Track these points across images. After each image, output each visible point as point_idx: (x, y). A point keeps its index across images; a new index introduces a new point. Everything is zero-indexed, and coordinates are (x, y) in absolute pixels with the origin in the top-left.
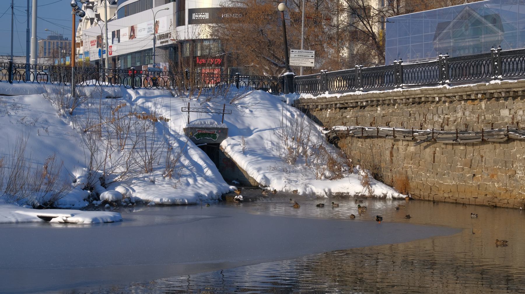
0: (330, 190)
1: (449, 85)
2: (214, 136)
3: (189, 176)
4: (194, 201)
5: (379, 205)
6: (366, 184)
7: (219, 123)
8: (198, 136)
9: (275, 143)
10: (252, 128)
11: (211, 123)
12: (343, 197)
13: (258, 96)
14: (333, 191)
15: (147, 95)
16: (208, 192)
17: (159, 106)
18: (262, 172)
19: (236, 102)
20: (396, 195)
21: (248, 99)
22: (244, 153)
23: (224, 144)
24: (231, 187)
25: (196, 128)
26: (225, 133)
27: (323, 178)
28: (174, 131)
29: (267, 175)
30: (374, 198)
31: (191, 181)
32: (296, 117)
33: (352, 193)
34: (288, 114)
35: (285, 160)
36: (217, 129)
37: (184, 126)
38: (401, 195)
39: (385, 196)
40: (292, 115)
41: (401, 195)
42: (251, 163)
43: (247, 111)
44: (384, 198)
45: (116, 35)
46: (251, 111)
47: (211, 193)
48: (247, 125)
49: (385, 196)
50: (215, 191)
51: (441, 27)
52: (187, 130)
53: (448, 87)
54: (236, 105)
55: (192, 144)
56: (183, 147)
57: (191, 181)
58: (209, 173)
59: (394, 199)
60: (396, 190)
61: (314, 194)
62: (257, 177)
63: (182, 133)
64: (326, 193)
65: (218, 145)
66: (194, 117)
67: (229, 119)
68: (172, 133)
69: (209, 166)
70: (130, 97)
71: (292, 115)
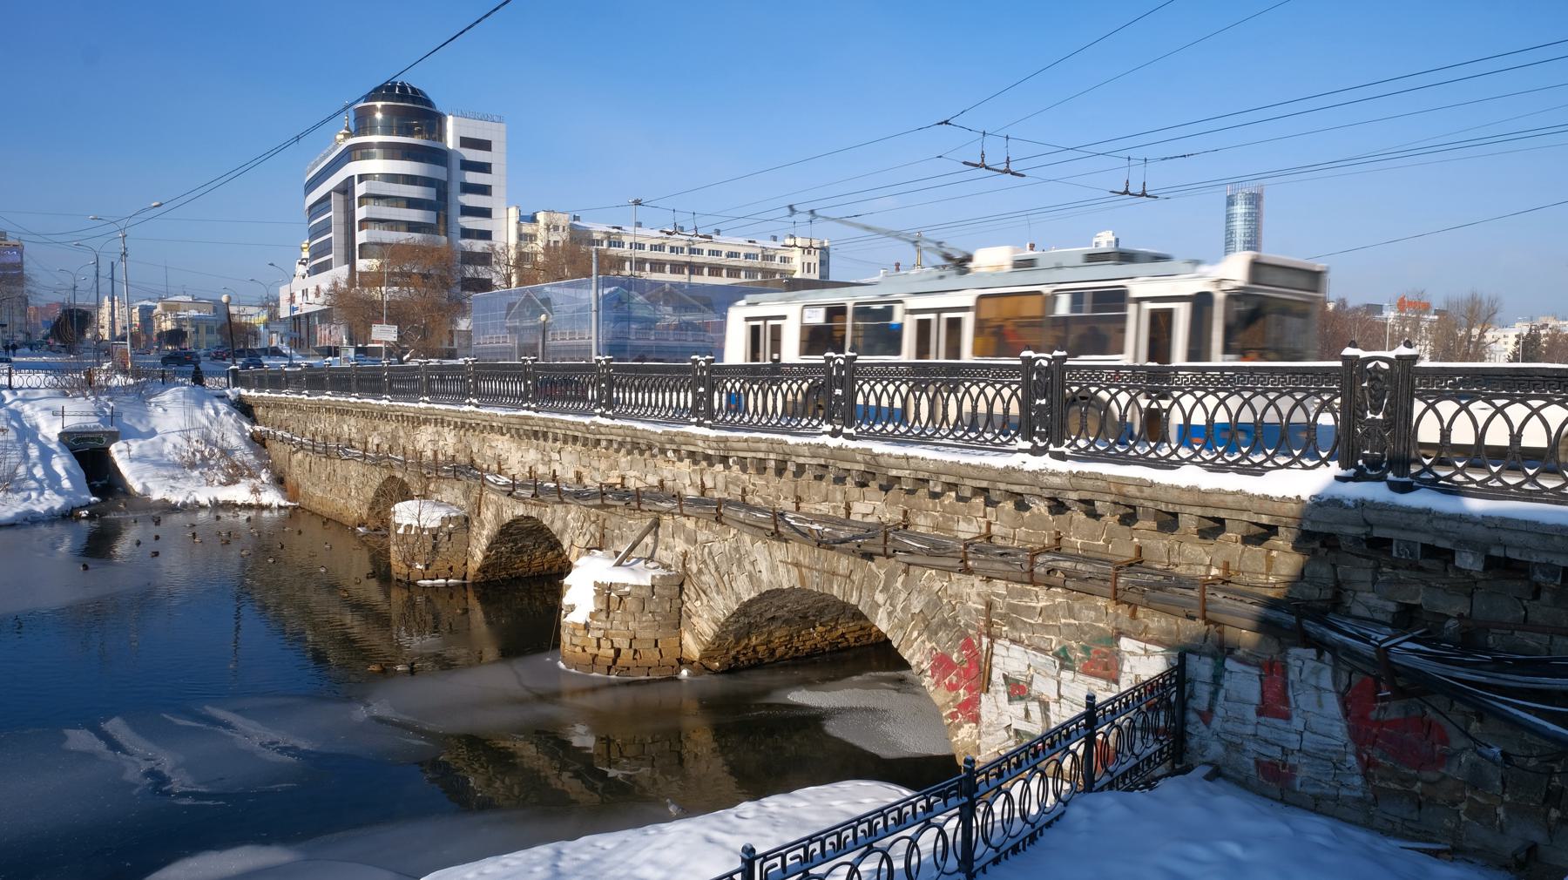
0: (215, 498)
1: (308, 396)
2: (100, 440)
3: (35, 489)
4: (13, 522)
5: (266, 514)
6: (255, 491)
7: (105, 427)
8: (77, 441)
9: (178, 446)
10: (158, 430)
11: (95, 427)
12: (229, 506)
13: (180, 394)
14: (219, 499)
15: (28, 397)
16: (46, 508)
17: (37, 409)
18: (142, 480)
19: (152, 400)
20: (283, 503)
21: (168, 396)
22: (131, 459)
23: (113, 448)
24: (93, 499)
25: (72, 433)
26: (114, 437)
27: (216, 483)
28: (44, 437)
29: (149, 485)
30: (261, 507)
31: (34, 495)
32: (222, 414)
33: (239, 502)
34: (212, 412)
35: (181, 466)
36: (103, 432)
37: (59, 430)
38: (288, 504)
39: (271, 504)
40: (217, 412)
41: (288, 504)
42: (133, 472)
43: (160, 410)
44: (268, 507)
45: (305, 292)
46: (165, 410)
47: (51, 509)
48: (152, 426)
49: (271, 504)
50: (57, 507)
51: (511, 306)
52: (61, 435)
53: (306, 397)
54: (150, 403)
55: (63, 451)
56: (46, 454)
57: (34, 495)
58: (66, 484)
59: (280, 507)
60: (284, 498)
61: (197, 502)
62: (137, 487)
63: (56, 439)
64: (210, 502)
65: (106, 451)
66: (71, 422)
67: (130, 420)
68: (40, 438)
69: (70, 477)
70: (4, 399)
71: (217, 412)
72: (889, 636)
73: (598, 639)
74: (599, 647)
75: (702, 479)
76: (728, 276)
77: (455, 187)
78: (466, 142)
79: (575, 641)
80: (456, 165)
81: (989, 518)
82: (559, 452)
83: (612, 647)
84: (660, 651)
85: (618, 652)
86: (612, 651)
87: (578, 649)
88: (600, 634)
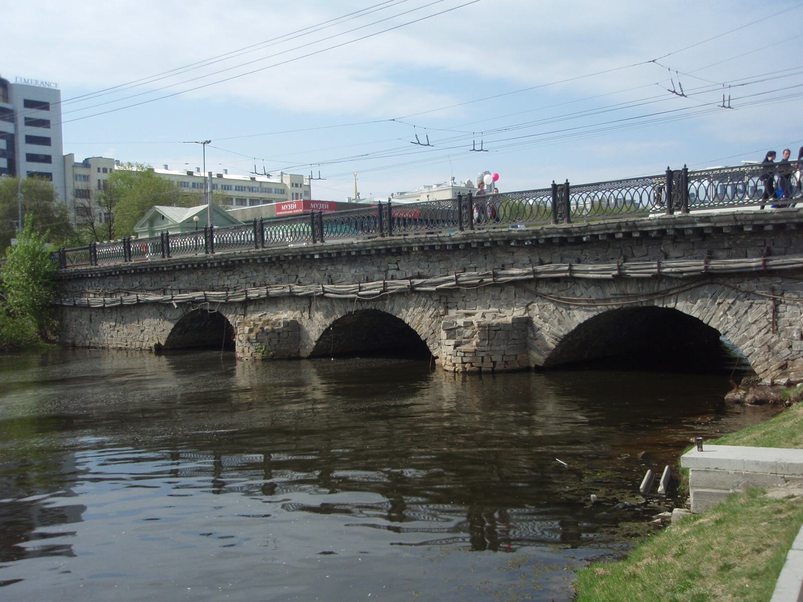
72: (700, 319)
73: (483, 357)
74: (483, 361)
75: (540, 259)
76: (236, 205)
77: (21, 141)
78: (29, 104)
79: (465, 360)
80: (21, 121)
81: (768, 245)
82: (397, 263)
83: (492, 361)
84: (518, 362)
85: (494, 363)
86: (492, 364)
87: (467, 366)
88: (483, 354)
